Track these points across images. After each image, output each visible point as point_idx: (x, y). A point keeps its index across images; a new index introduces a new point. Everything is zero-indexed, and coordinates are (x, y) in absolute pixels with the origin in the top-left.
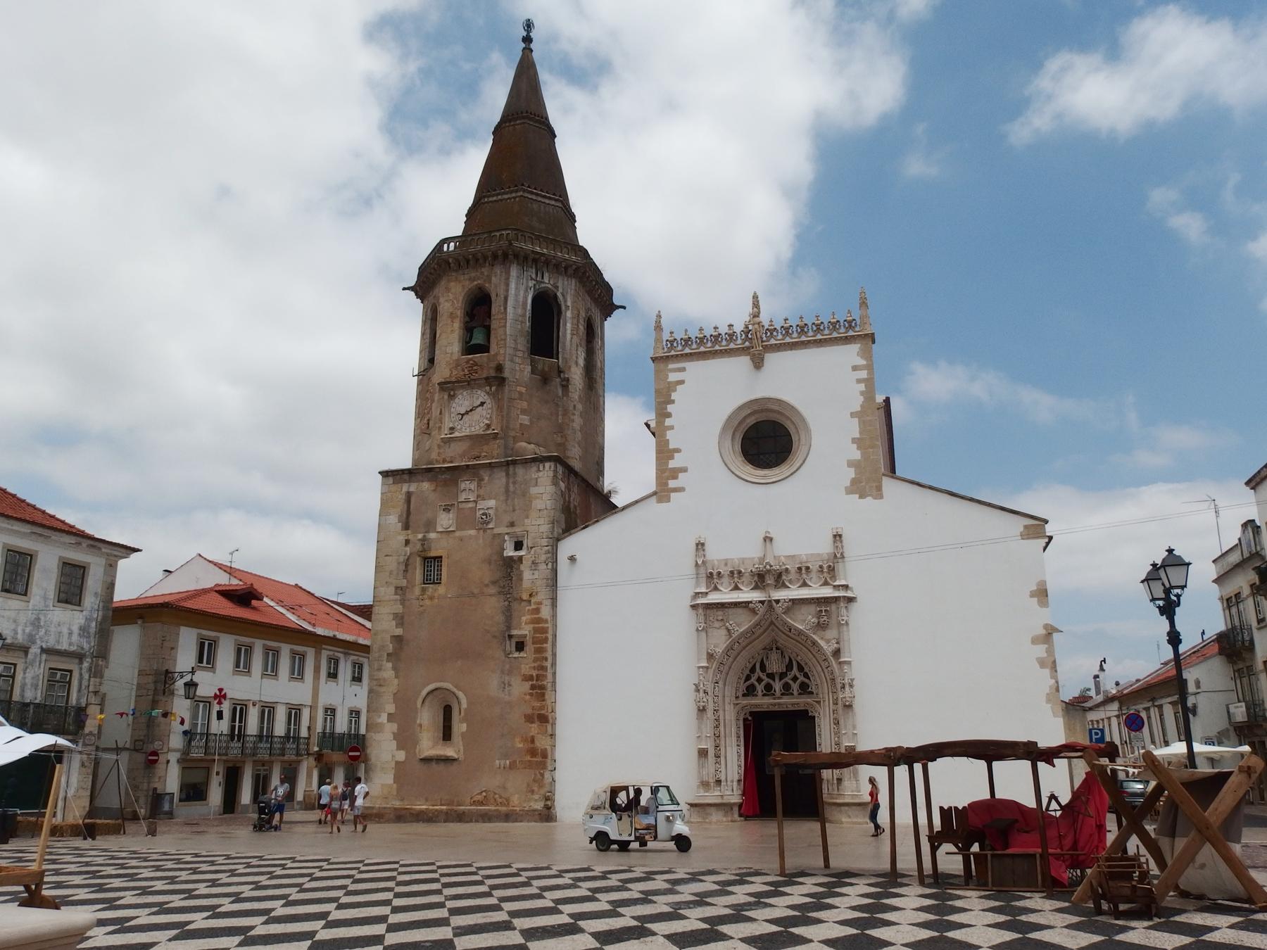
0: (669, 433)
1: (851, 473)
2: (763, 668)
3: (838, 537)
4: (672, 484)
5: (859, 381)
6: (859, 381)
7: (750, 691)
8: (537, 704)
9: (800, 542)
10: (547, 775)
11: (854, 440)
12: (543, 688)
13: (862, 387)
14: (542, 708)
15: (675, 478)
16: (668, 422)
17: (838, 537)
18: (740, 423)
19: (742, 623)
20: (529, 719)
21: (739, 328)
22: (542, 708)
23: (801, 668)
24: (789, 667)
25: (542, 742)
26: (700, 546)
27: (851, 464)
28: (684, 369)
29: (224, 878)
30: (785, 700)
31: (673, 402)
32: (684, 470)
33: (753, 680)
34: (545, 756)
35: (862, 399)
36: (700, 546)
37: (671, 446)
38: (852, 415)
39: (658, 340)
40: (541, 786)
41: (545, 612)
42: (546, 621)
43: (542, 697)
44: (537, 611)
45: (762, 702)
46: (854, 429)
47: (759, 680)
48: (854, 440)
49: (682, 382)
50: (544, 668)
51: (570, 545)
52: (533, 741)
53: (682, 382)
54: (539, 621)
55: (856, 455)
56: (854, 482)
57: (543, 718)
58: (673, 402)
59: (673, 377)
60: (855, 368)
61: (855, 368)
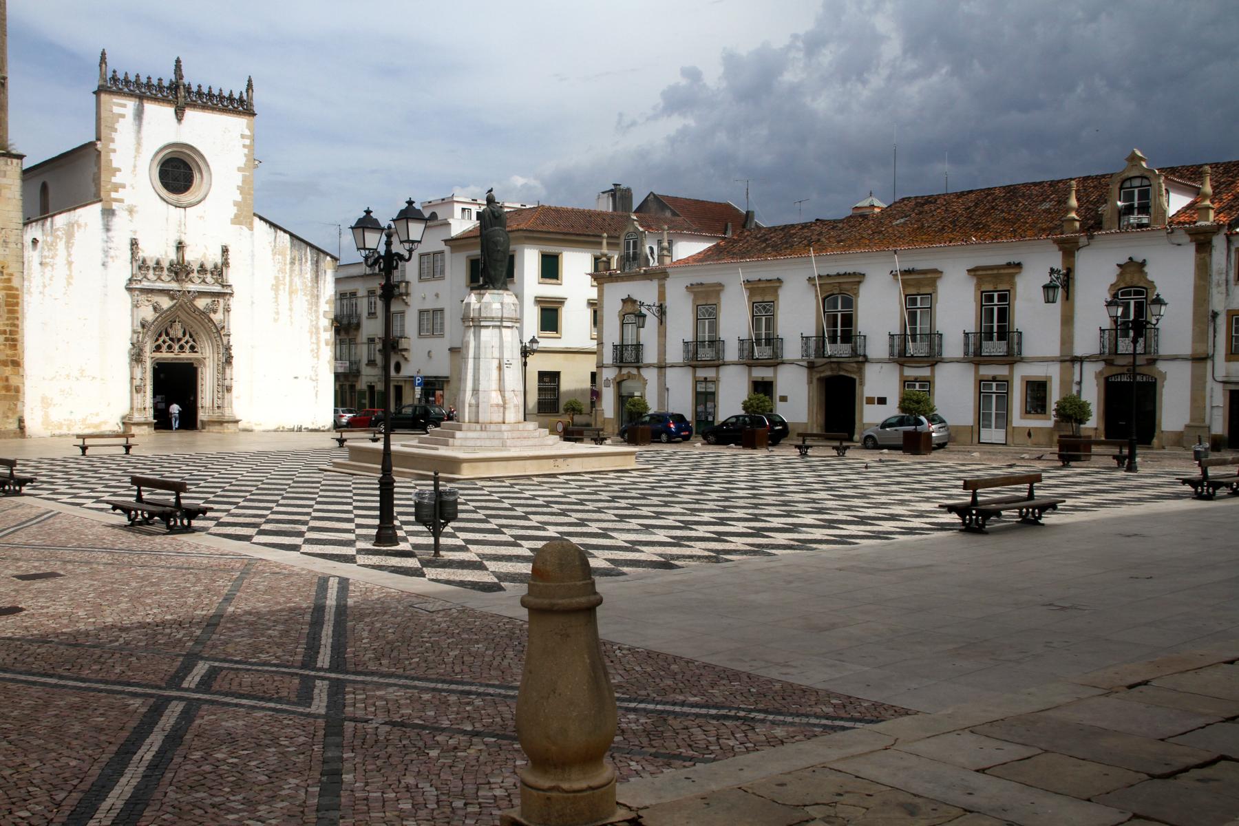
0: (112, 155)
1: (234, 210)
2: (167, 334)
3: (225, 251)
4: (114, 195)
5: (244, 146)
6: (244, 146)
7: (158, 348)
8: (9, 352)
9: (201, 252)
10: (19, 404)
11: (239, 188)
12: (14, 340)
13: (246, 151)
14: (14, 355)
15: (117, 191)
16: (112, 146)
17: (225, 251)
18: (157, 153)
19: (166, 303)
20: (5, 363)
21: (166, 83)
22: (14, 355)
23: (191, 336)
24: (184, 335)
25: (14, 381)
26: (134, 244)
27: (236, 204)
28: (124, 106)
29: (157, 468)
30: (183, 355)
31: (115, 130)
32: (123, 186)
33: (160, 342)
34: (17, 390)
35: (244, 159)
36: (134, 244)
37: (115, 165)
38: (239, 169)
39: (103, 75)
40: (14, 413)
41: (15, 283)
42: (17, 289)
43: (14, 347)
44: (9, 280)
45: (165, 355)
46: (238, 179)
47: (164, 342)
48: (239, 188)
49: (123, 116)
50: (16, 326)
51: (34, 231)
52: (7, 379)
53: (123, 116)
54: (11, 288)
55: (239, 198)
56: (236, 216)
57: (16, 364)
58: (115, 130)
59: (116, 110)
60: (243, 136)
61: (243, 136)
